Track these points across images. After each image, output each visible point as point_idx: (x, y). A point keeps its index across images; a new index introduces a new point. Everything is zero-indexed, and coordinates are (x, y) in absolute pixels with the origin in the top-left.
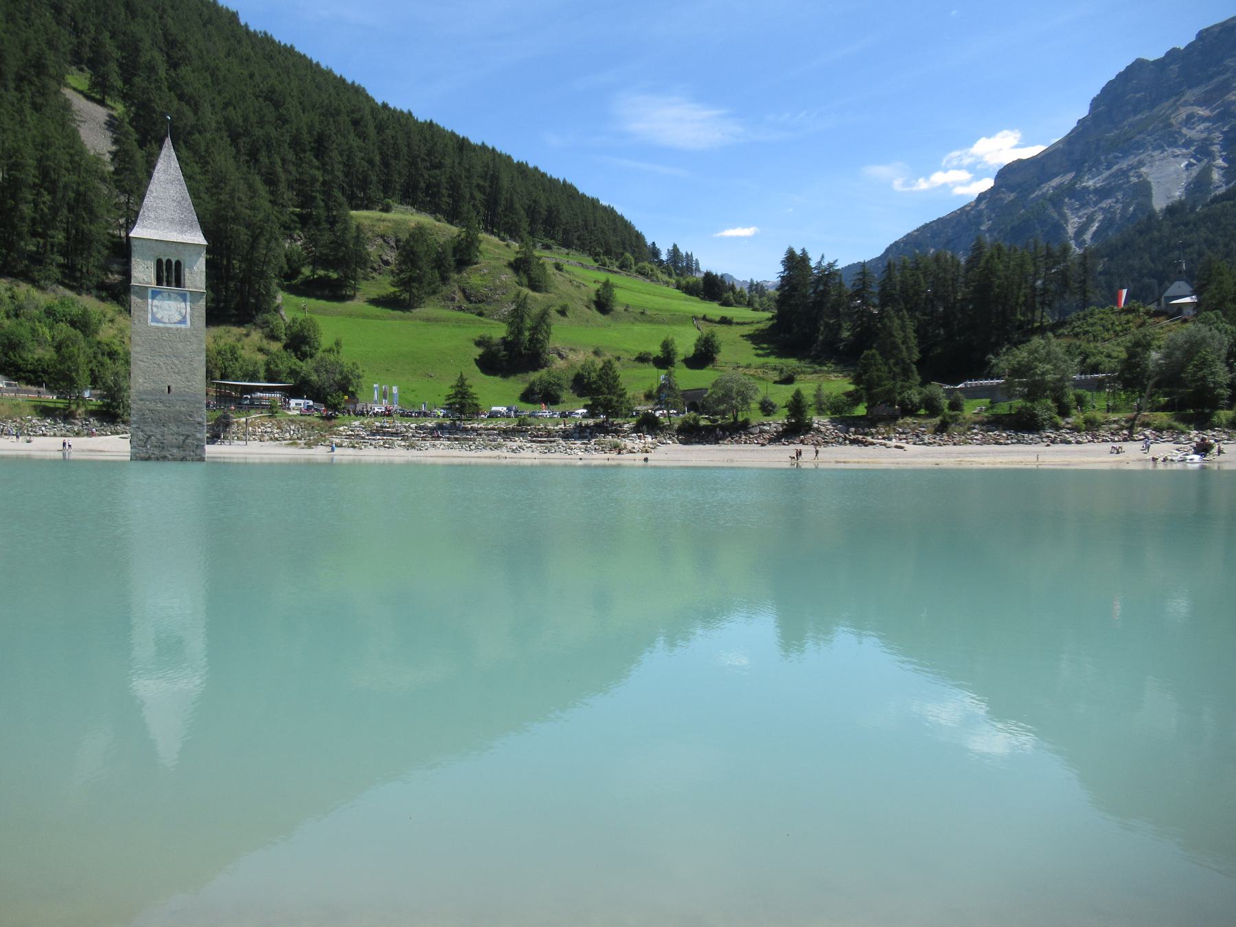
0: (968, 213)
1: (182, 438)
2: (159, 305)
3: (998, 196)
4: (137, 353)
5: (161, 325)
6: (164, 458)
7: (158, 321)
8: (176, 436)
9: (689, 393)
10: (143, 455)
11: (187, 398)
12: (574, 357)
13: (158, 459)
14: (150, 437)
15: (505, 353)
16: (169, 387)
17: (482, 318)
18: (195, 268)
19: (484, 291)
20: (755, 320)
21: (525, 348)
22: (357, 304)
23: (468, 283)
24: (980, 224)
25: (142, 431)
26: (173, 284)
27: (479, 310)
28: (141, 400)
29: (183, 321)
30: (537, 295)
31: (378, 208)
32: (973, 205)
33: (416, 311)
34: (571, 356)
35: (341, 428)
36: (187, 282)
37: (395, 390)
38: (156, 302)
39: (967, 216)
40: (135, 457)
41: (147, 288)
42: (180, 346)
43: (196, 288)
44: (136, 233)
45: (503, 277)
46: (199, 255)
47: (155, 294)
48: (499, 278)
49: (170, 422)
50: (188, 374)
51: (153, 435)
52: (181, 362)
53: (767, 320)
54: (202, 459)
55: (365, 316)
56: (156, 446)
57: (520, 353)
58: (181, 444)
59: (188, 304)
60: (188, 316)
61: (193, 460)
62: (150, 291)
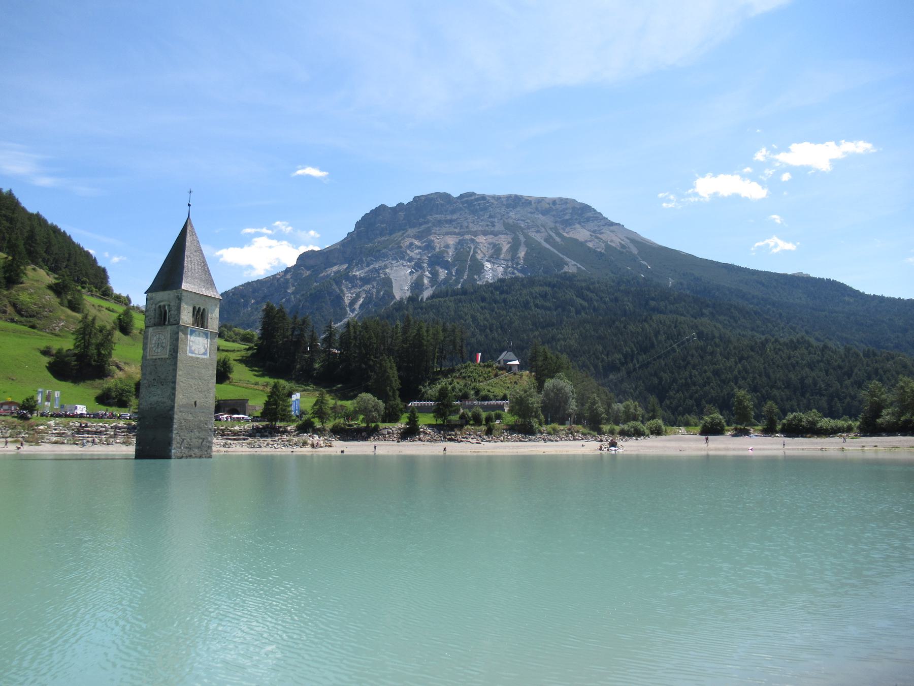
0: (278, 280)
1: (201, 440)
2: (194, 340)
3: (299, 272)
4: (179, 375)
5: (194, 355)
6: (191, 456)
8: (197, 440)
10: (179, 455)
11: (205, 411)
12: (129, 369)
13: (187, 457)
14: (183, 440)
15: (76, 363)
16: (195, 402)
17: (36, 331)
18: (214, 315)
19: (34, 308)
20: (236, 349)
21: (94, 361)
23: (18, 299)
24: (288, 288)
25: (179, 436)
26: (200, 325)
27: (31, 324)
28: (180, 412)
29: (205, 354)
32: (281, 274)
34: (127, 368)
35: (41, 427)
36: (209, 326)
37: (57, 394)
38: (192, 338)
39: (277, 281)
41: (188, 327)
42: (203, 371)
45: (47, 297)
46: (216, 305)
47: (192, 332)
48: (44, 298)
49: (195, 429)
50: (206, 393)
51: (185, 439)
53: (245, 349)
54: (210, 457)
57: (90, 365)
59: (209, 340)
60: (208, 350)
61: (206, 457)
62: (189, 329)
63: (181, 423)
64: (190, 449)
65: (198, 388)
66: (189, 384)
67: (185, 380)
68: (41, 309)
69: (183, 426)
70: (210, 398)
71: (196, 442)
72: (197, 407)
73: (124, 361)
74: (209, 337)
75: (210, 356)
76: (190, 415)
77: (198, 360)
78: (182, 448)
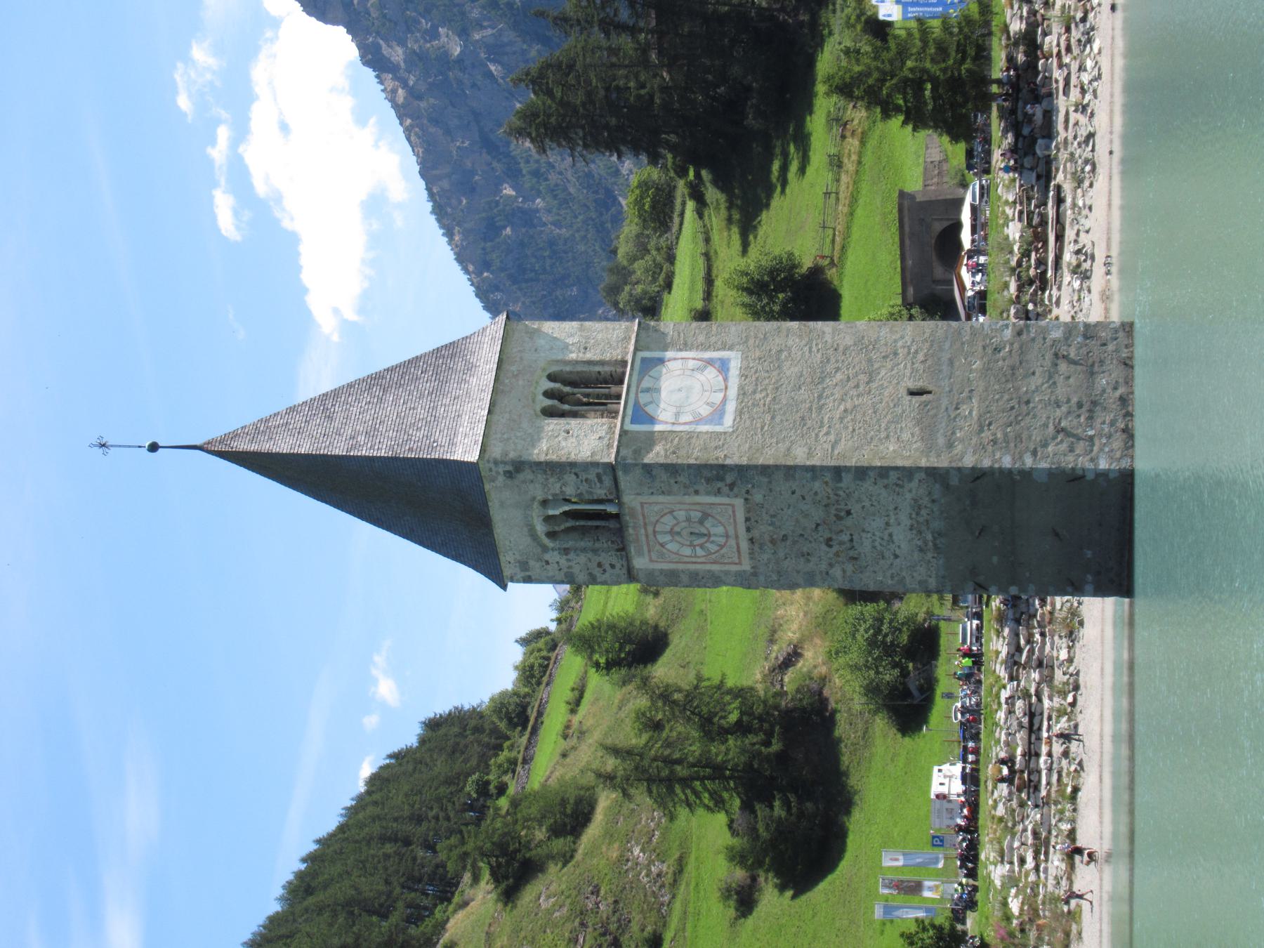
0: (413, 94)
1: (1063, 367)
3: (374, 14)
4: (810, 455)
5: (731, 407)
6: (1124, 401)
7: (719, 413)
9: (910, 262)
10: (1117, 443)
11: (946, 356)
12: (795, 626)
13: (1129, 415)
14: (1060, 430)
17: (668, 936)
18: (570, 341)
20: (701, 247)
21: (767, 743)
24: (444, 56)
25: (1045, 445)
26: (614, 389)
28: (950, 445)
29: (723, 367)
30: (599, 816)
32: (390, 84)
34: (790, 634)
35: (1015, 906)
37: (893, 861)
39: (420, 98)
41: (623, 433)
42: (790, 371)
43: (627, 339)
45: (545, 904)
46: (533, 334)
47: (642, 415)
48: (550, 912)
49: (1017, 389)
50: (874, 355)
52: (838, 369)
53: (700, 216)
56: (1090, 418)
57: (782, 757)
58: (1079, 368)
59: (669, 354)
62: (630, 427)
63: (995, 442)
64: (1094, 403)
65: (857, 386)
66: (841, 419)
67: (827, 434)
68: (590, 921)
69: (1006, 435)
70: (896, 341)
71: (1069, 384)
72: (930, 388)
73: (762, 644)
75: (731, 348)
76: (965, 411)
77: (750, 389)
78: (1091, 433)
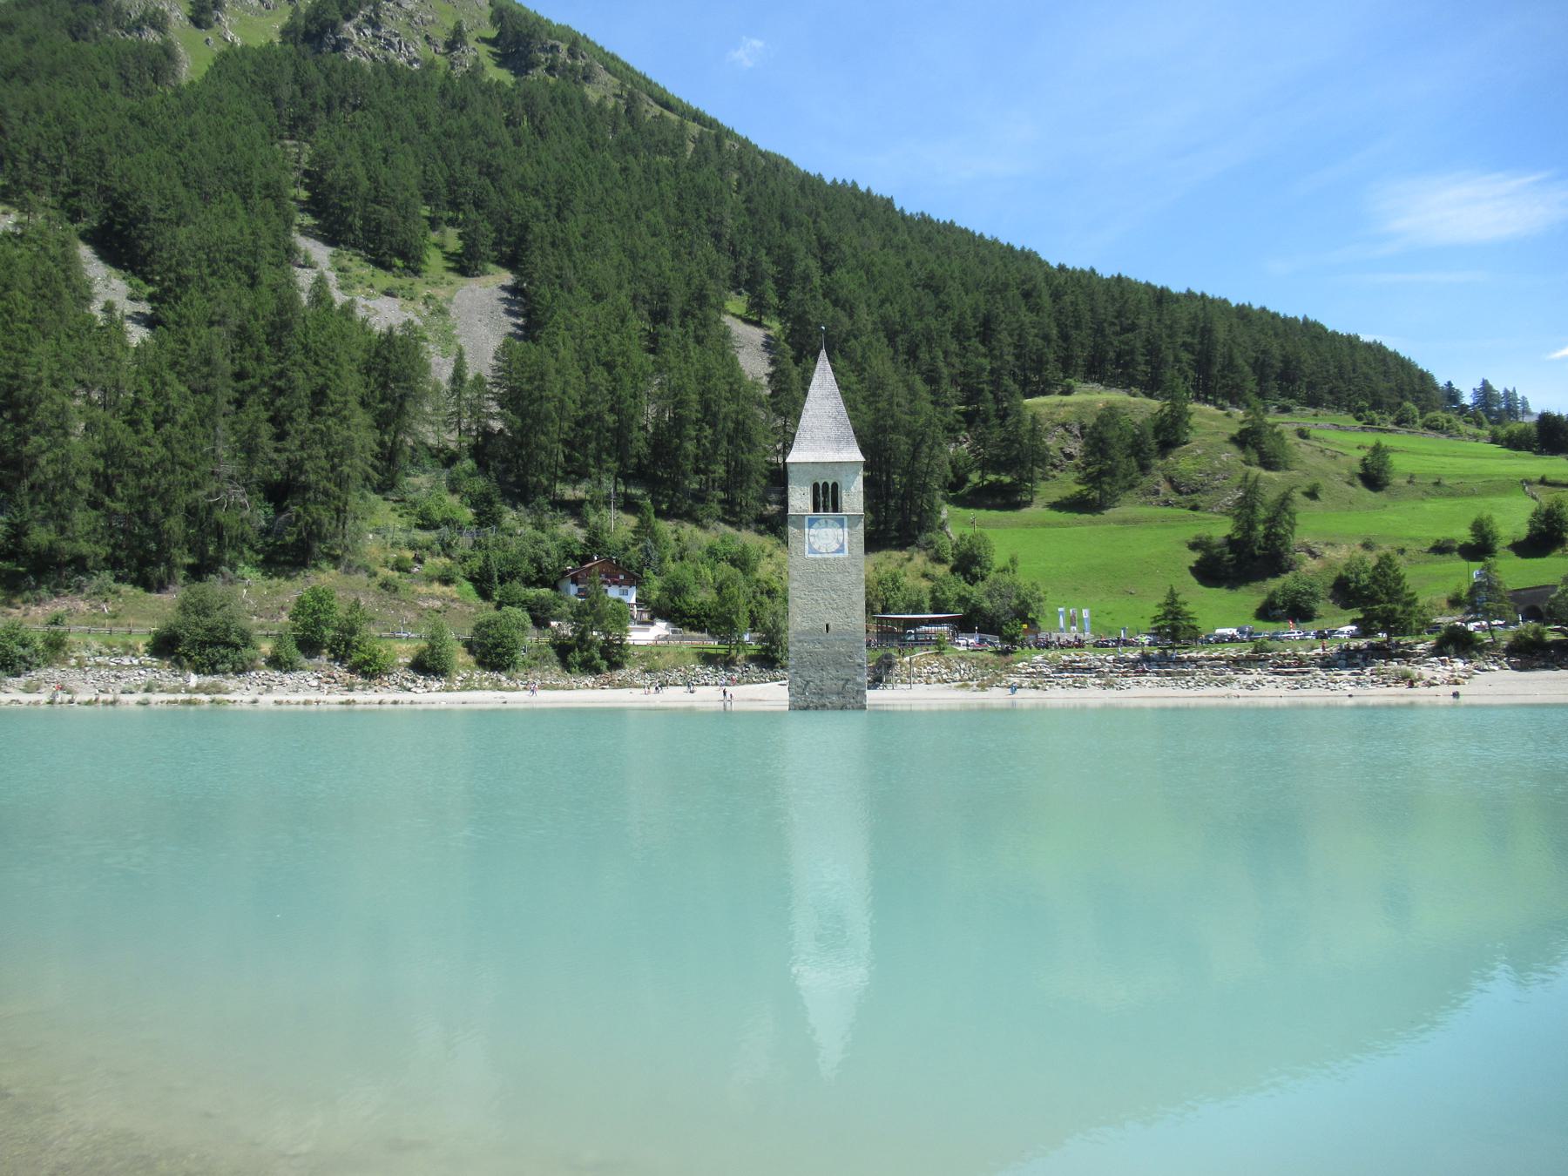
1: (842, 683)
4: (794, 589)
5: (818, 556)
6: (824, 706)
7: (815, 552)
9: (1523, 593)
10: (801, 704)
11: (846, 637)
12: (1333, 554)
13: (817, 708)
14: (808, 682)
15: (1231, 556)
16: (827, 626)
17: (1197, 513)
19: (1197, 477)
21: (1260, 548)
22: (1036, 511)
26: (830, 509)
27: (1192, 504)
28: (799, 641)
29: (841, 550)
30: (1273, 474)
31: (1057, 392)
33: (1108, 513)
35: (1020, 665)
37: (1085, 613)
38: (813, 531)
40: (794, 707)
41: (804, 516)
42: (838, 578)
44: (793, 457)
47: (812, 522)
48: (1218, 459)
50: (847, 610)
54: (863, 707)
55: (1046, 525)
57: (1253, 556)
59: (846, 529)
61: (853, 708)
64: (822, 695)
68: (1211, 477)
73: (1325, 540)
74: (846, 524)
76: (818, 646)
